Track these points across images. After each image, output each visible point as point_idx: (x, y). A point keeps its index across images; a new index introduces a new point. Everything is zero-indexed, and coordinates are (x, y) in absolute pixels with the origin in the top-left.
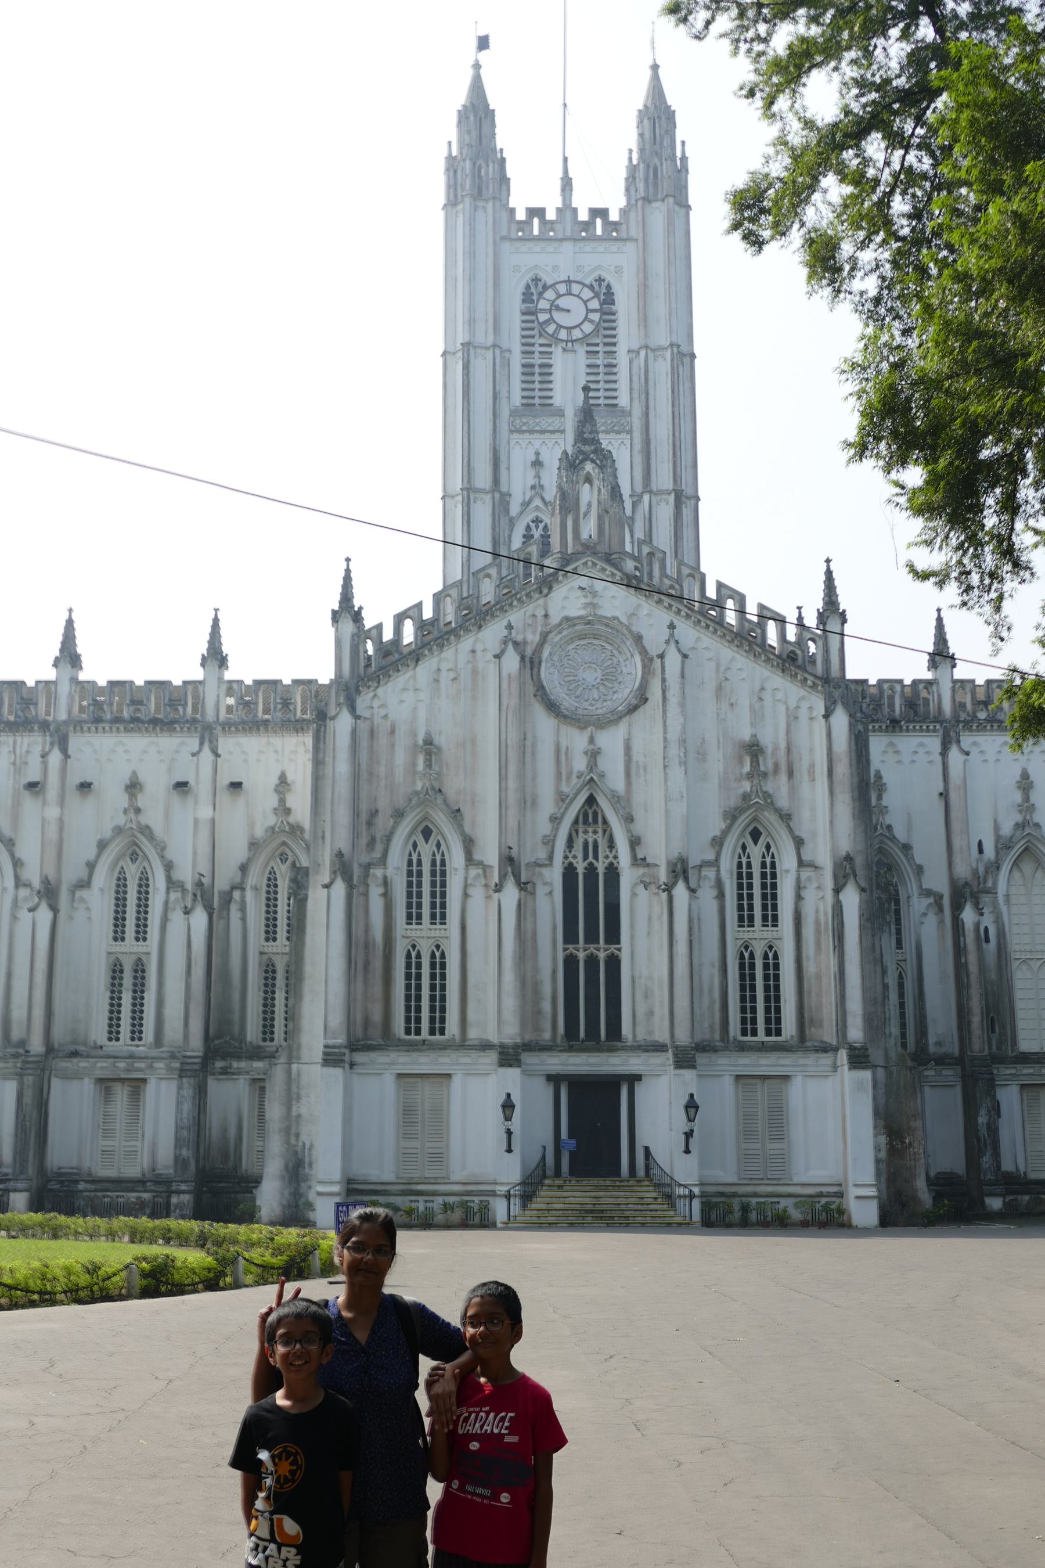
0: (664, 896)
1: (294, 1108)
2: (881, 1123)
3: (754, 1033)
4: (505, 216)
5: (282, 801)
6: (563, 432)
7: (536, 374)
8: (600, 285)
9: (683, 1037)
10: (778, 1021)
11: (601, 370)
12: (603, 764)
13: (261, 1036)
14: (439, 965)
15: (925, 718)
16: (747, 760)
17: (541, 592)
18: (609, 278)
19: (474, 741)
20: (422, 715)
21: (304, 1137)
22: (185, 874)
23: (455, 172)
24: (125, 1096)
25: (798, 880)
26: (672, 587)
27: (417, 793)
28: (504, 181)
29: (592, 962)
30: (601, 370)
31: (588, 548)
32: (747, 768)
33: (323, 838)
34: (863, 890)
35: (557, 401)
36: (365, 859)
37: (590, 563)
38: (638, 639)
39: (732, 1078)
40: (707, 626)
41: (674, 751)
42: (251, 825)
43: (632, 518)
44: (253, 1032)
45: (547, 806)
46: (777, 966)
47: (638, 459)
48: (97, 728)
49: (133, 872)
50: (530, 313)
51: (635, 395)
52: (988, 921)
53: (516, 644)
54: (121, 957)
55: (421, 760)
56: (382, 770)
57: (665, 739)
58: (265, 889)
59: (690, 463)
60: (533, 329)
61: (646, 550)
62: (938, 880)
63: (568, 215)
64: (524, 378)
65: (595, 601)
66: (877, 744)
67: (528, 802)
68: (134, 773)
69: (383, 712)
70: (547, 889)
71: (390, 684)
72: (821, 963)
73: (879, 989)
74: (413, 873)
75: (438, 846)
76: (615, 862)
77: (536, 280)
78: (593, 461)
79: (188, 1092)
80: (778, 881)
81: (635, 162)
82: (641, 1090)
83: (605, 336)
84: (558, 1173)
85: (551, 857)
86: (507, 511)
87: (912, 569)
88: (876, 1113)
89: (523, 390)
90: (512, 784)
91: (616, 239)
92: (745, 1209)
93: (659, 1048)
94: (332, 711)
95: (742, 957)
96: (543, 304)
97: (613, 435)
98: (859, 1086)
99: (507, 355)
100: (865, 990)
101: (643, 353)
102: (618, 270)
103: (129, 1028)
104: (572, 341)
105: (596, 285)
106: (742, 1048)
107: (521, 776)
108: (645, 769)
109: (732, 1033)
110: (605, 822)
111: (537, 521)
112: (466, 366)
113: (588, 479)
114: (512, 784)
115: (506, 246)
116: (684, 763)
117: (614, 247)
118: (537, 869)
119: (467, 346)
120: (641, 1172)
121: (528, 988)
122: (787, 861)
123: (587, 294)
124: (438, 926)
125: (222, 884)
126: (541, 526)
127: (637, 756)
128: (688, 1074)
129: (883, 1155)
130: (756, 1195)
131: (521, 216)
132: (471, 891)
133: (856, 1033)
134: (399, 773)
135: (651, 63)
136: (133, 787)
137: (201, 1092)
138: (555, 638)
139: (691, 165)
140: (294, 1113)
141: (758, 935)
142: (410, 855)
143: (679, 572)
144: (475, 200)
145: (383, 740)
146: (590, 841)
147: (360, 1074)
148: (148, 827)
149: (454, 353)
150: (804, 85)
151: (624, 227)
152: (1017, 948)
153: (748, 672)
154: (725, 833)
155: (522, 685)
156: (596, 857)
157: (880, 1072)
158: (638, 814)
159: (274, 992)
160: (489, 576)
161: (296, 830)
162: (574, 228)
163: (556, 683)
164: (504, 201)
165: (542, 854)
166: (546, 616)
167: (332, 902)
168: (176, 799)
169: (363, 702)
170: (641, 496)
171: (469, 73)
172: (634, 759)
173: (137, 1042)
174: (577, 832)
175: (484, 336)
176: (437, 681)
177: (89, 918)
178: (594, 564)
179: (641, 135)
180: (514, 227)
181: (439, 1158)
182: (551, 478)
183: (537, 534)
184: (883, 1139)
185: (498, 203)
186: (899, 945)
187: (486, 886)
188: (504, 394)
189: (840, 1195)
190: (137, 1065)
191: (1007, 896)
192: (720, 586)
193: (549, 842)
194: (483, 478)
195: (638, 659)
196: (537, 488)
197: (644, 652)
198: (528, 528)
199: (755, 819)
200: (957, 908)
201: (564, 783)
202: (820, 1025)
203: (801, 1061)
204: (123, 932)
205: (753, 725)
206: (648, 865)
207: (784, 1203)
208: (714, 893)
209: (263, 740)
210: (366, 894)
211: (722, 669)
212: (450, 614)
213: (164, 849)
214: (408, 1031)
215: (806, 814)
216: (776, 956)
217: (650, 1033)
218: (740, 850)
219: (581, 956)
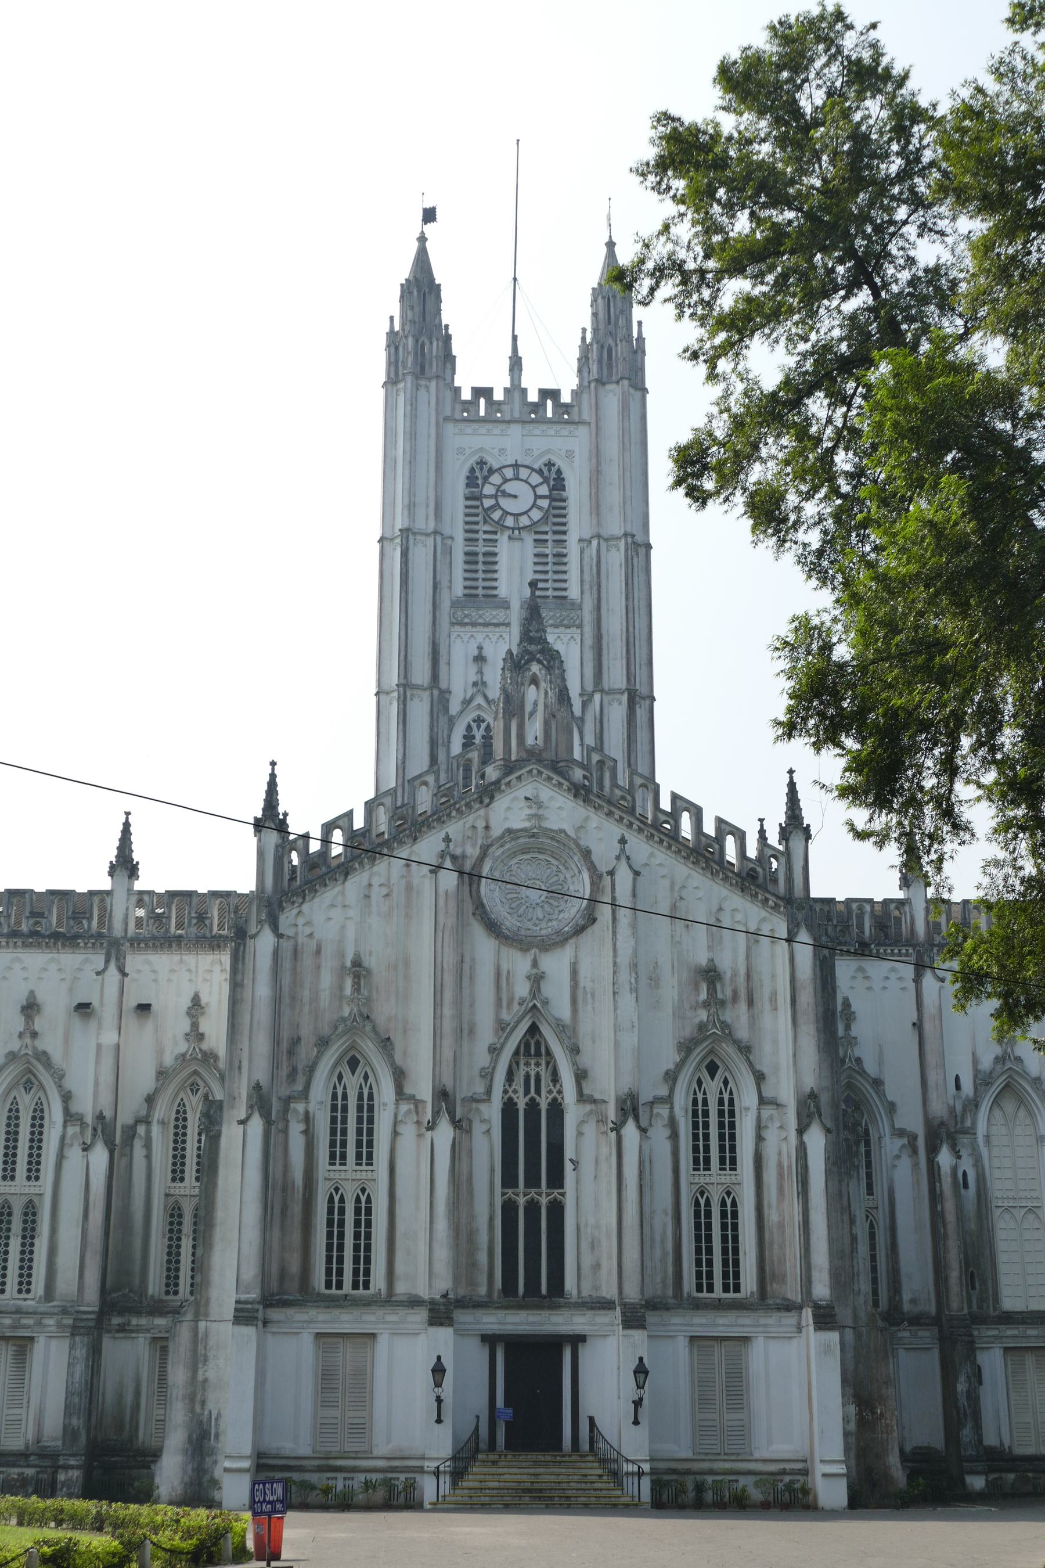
0: (613, 1135)
1: (200, 1372)
2: (850, 1391)
3: (710, 1289)
4: (449, 395)
5: (195, 1025)
6: (508, 625)
7: (481, 563)
8: (550, 470)
9: (632, 1293)
10: (737, 1275)
11: (550, 559)
12: (548, 989)
13: (164, 1289)
14: (364, 1211)
15: (897, 941)
16: (704, 987)
17: (481, 802)
18: (559, 462)
19: (407, 964)
20: (351, 934)
21: (210, 1405)
22: (85, 1106)
23: (397, 348)
24: (10, 1353)
25: (759, 1119)
26: (623, 798)
27: (344, 1020)
28: (449, 359)
29: (533, 1207)
30: (550, 559)
31: (533, 755)
32: (703, 996)
33: (240, 1068)
34: (828, 1131)
35: (503, 591)
36: (284, 1091)
37: (535, 772)
38: (587, 854)
39: (687, 1340)
40: (661, 841)
41: (624, 976)
42: (160, 1052)
43: (582, 719)
44: (155, 1285)
45: (486, 1035)
46: (735, 1215)
47: (589, 655)
49: (26, 1102)
50: (474, 497)
51: (587, 587)
52: (966, 1164)
53: (454, 858)
54: (8, 1197)
55: (349, 983)
56: (306, 994)
57: (615, 963)
58: (173, 1123)
59: (644, 661)
60: (477, 515)
61: (595, 758)
62: (911, 1119)
63: (517, 395)
64: (467, 567)
65: (541, 812)
66: (844, 969)
67: (465, 1031)
68: (32, 992)
69: (308, 930)
70: (484, 1127)
71: (316, 900)
72: (783, 1211)
73: (847, 1240)
74: (338, 1108)
75: (366, 1077)
76: (559, 1098)
77: (482, 463)
78: (540, 662)
79: (81, 1352)
80: (737, 1119)
81: (588, 340)
82: (585, 1353)
83: (555, 524)
84: (492, 1446)
85: (489, 1092)
86: (446, 709)
87: (852, 828)
88: (844, 1381)
89: (465, 579)
90: (447, 1011)
91: (567, 422)
92: (700, 1488)
93: (606, 1305)
94: (253, 929)
95: (697, 1203)
96: (489, 490)
97: (562, 629)
98: (826, 1350)
99: (449, 542)
100: (831, 1240)
101: (595, 542)
102: (570, 455)
103: (17, 1280)
104: (519, 529)
105: (545, 470)
106: (697, 1306)
107: (458, 1003)
108: (593, 995)
109: (686, 1289)
110: (549, 1053)
111: (479, 720)
112: (405, 554)
113: (534, 681)
114: (447, 1011)
115: (450, 428)
116: (635, 990)
117: (566, 430)
118: (474, 1105)
119: (406, 532)
120: (585, 1446)
121: (462, 1235)
122: (747, 1098)
123: (536, 479)
124: (364, 1167)
125: (125, 1118)
126: (483, 726)
127: (584, 981)
128: (638, 1336)
129: (852, 1426)
130: (711, 1472)
131: (466, 395)
132: (401, 1129)
133: (822, 1290)
134: (325, 996)
135: (607, 240)
136: (30, 1008)
137: (95, 1351)
138: (496, 852)
139: (648, 347)
140: (200, 1377)
141: (715, 1179)
142: (335, 1088)
143: (631, 782)
144: (417, 378)
145: (307, 961)
146: (533, 1073)
147: (274, 1333)
148: (44, 1053)
149: (392, 540)
150: (747, 347)
151: (576, 409)
152: (999, 1194)
153: (705, 893)
154: (680, 1066)
155: (460, 903)
156: (538, 1091)
157: (849, 1334)
158: (585, 1045)
159: (179, 1239)
160: (426, 783)
161: (209, 1058)
162: (522, 409)
163: (497, 901)
164: (448, 380)
165: (480, 1088)
166: (487, 828)
167: (249, 1139)
168: (77, 1022)
169: (286, 919)
170: (592, 695)
171: (415, 246)
172: (582, 985)
173: (24, 1295)
174: (518, 1064)
175: (425, 522)
176: (367, 897)
178: (540, 773)
179: (595, 315)
180: (458, 407)
181: (362, 1429)
182: (494, 676)
183: (478, 735)
184: (852, 1409)
185: (441, 383)
186: (870, 1190)
187: (418, 1122)
188: (445, 583)
189: (805, 1472)
190: (24, 1321)
191: (987, 1137)
192: (675, 797)
193: (487, 1075)
194: (421, 674)
195: (586, 875)
196: (480, 685)
197: (592, 868)
198: (469, 728)
199: (712, 1051)
200: (933, 1150)
201: (504, 1010)
202: (783, 1279)
203: (762, 1321)
205: (710, 948)
206: (595, 1101)
207: (743, 1481)
208: (667, 1132)
209: (176, 958)
210: (285, 1131)
211: (677, 888)
212: (383, 822)
213: (62, 1077)
214: (328, 1285)
215: (767, 1048)
216: (734, 1204)
217: (597, 1288)
218: (695, 1085)
219: (522, 1201)
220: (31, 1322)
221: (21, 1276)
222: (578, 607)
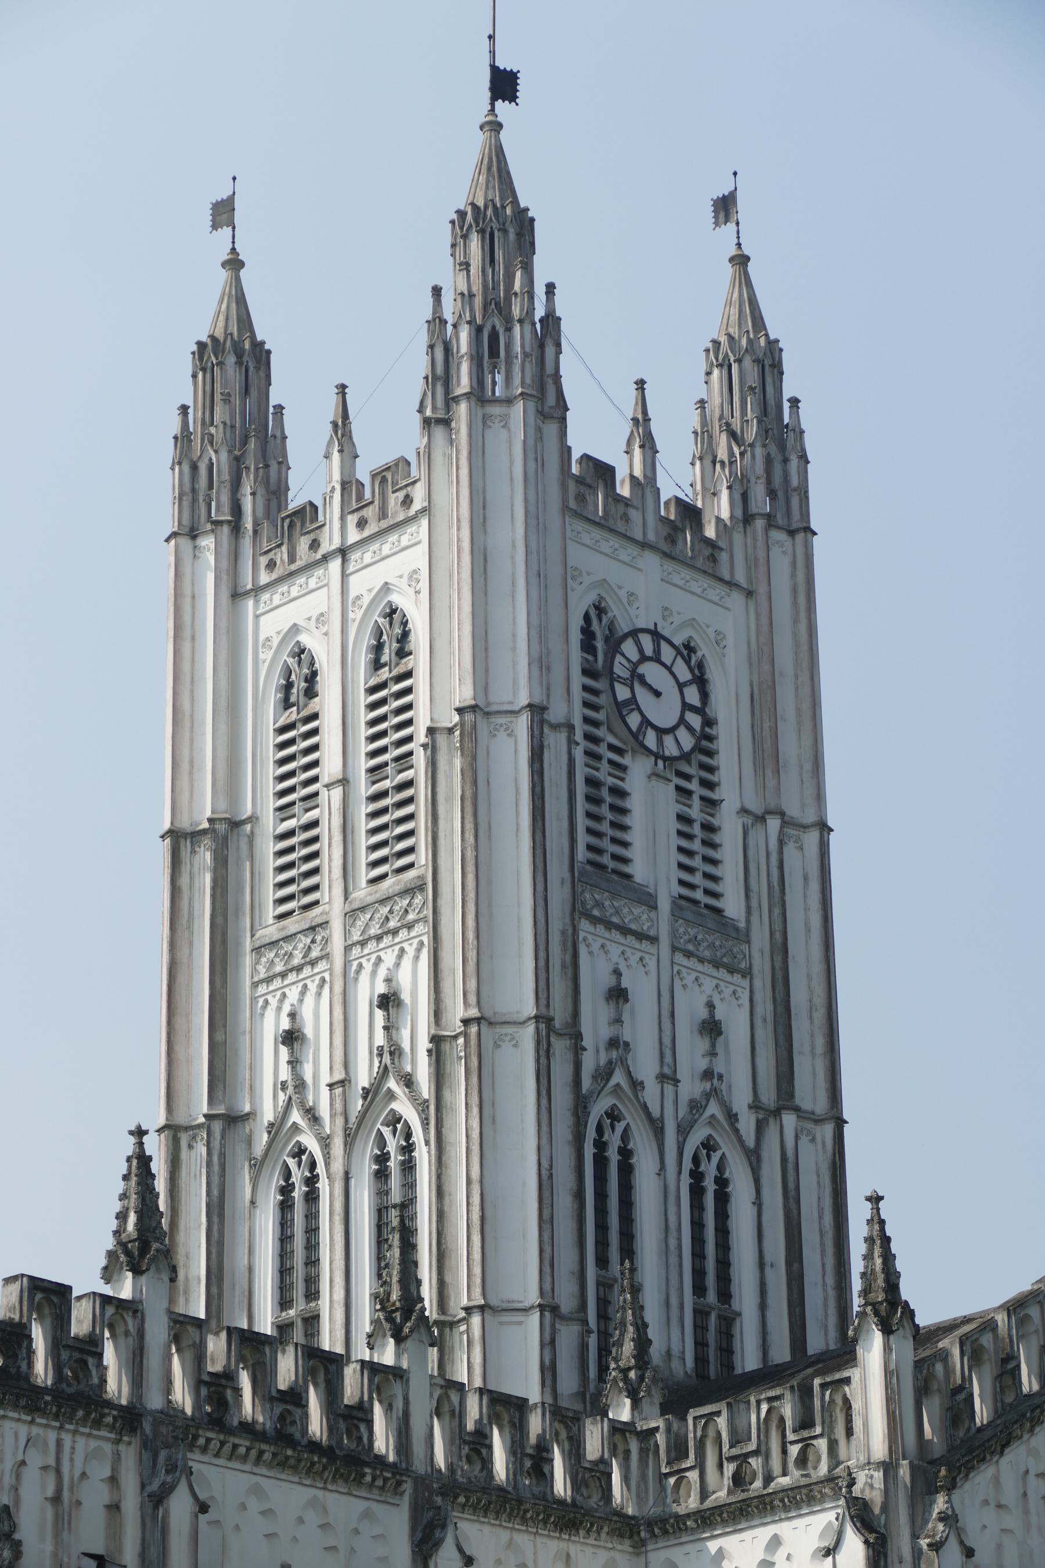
6: (654, 940)
30: (697, 829)
35: (639, 870)
47: (765, 1036)
71: (967, 1486)
77: (600, 609)
97: (722, 973)
104: (665, 759)
209: (504, 1535)
222: (745, 937)
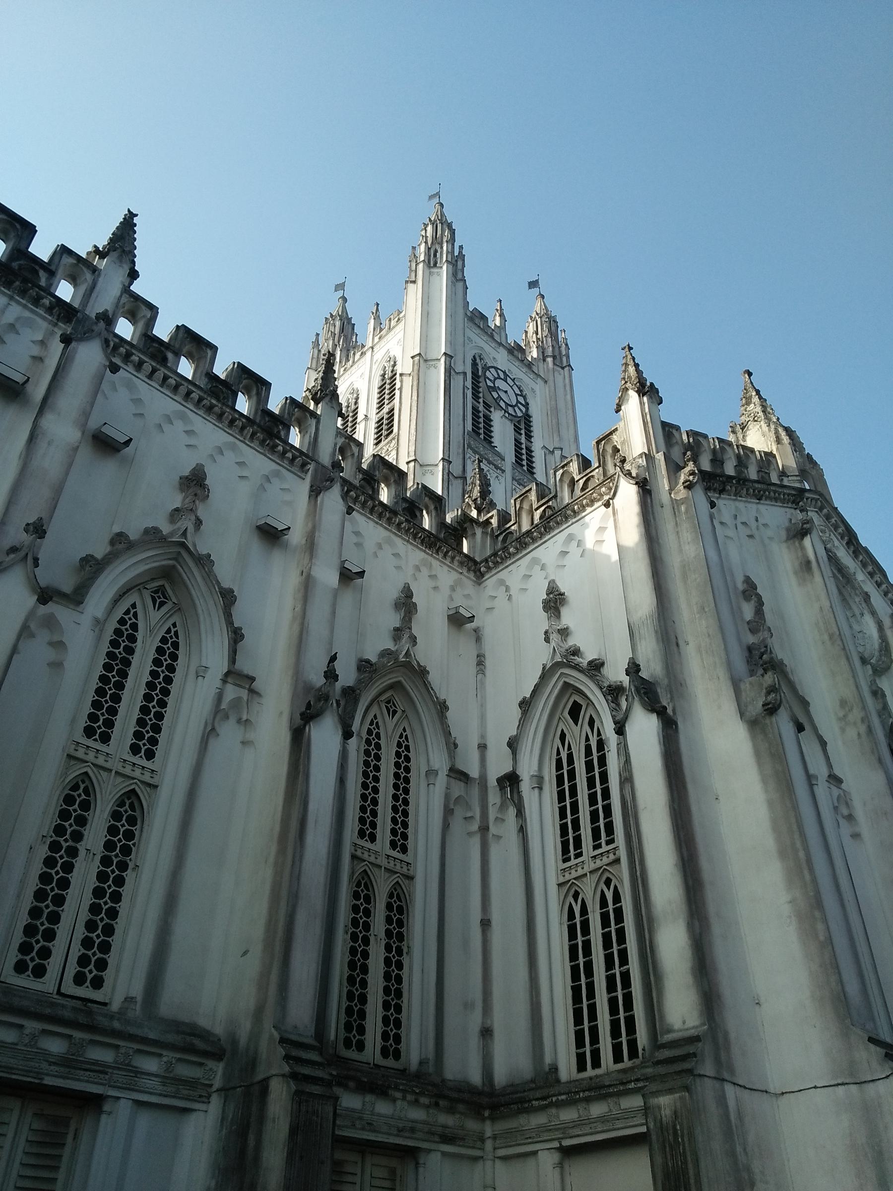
13: (342, 1034)
48: (154, 371)
177: (57, 666)
195: (868, 620)
204: (110, 724)
220: (105, 1056)
221: (87, 943)
